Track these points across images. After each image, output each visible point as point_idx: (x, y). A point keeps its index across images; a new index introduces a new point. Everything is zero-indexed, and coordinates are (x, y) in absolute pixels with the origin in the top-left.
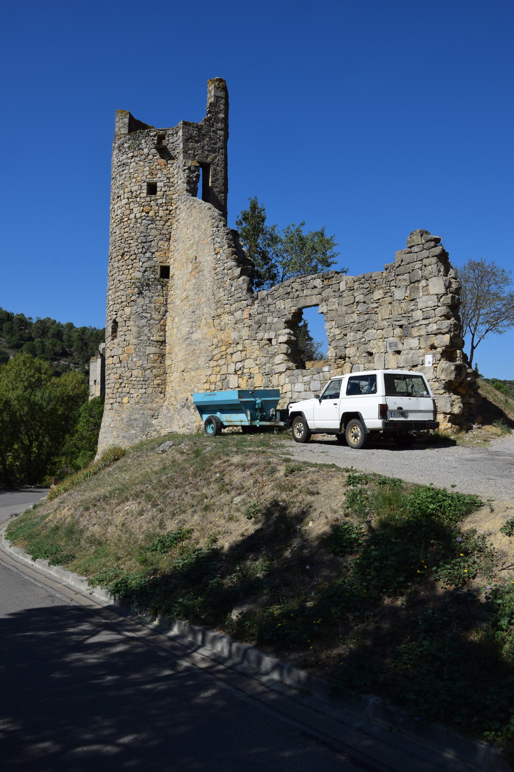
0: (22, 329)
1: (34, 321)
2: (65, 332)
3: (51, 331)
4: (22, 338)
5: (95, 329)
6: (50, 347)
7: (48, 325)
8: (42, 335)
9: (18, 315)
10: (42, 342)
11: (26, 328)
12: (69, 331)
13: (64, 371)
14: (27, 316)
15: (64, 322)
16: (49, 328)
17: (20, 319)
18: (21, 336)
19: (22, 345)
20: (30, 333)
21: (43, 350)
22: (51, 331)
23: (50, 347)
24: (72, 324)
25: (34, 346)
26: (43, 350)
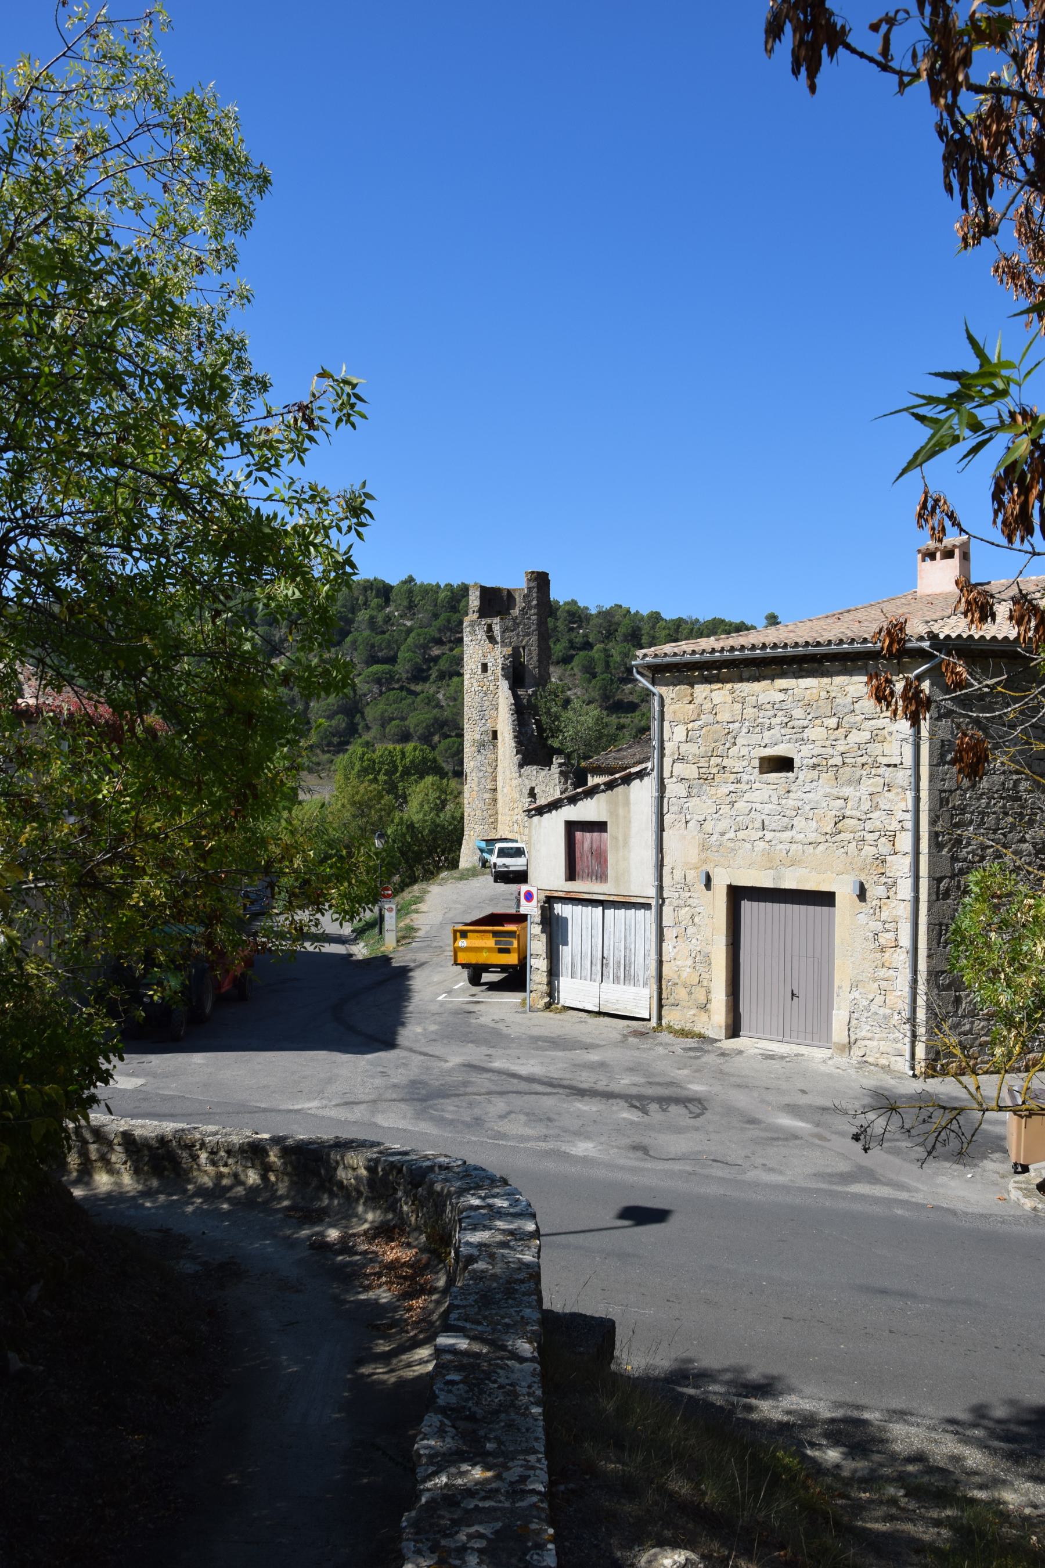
0: (572, 629)
1: (593, 611)
2: (646, 628)
3: (622, 630)
4: (572, 645)
5: (697, 620)
6: (618, 659)
7: (617, 618)
8: (607, 637)
9: (566, 603)
10: (605, 650)
11: (580, 627)
12: (653, 627)
13: (643, 701)
14: (581, 604)
15: (645, 612)
16: (618, 624)
17: (568, 612)
18: (571, 641)
19: (572, 657)
20: (586, 636)
21: (607, 665)
22: (622, 630)
23: (618, 659)
24: (658, 613)
25: (593, 659)
26: (607, 665)
